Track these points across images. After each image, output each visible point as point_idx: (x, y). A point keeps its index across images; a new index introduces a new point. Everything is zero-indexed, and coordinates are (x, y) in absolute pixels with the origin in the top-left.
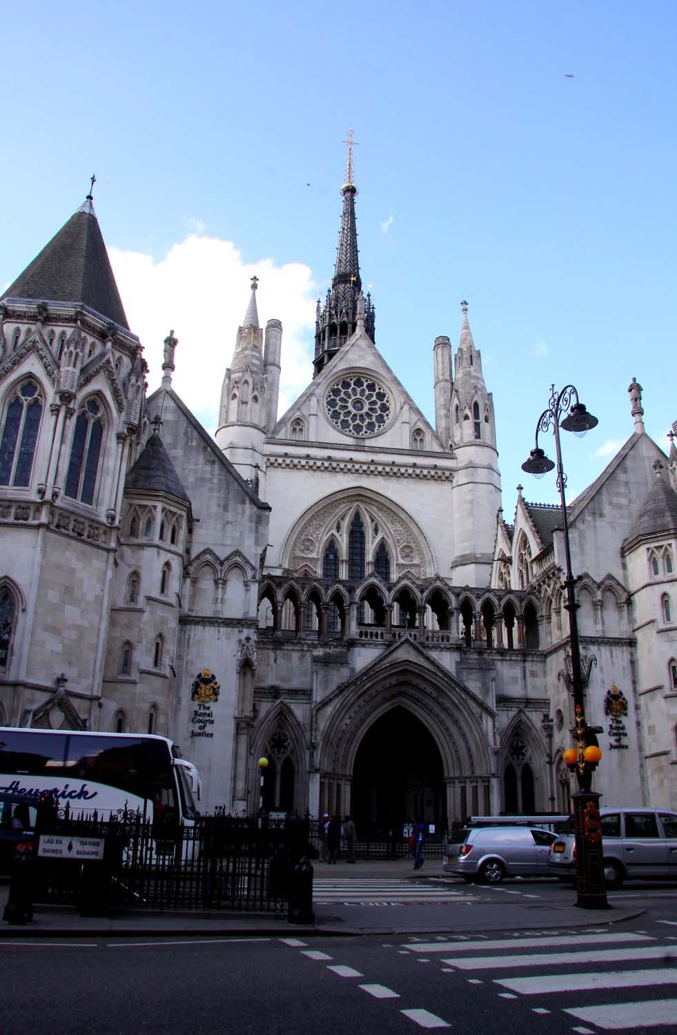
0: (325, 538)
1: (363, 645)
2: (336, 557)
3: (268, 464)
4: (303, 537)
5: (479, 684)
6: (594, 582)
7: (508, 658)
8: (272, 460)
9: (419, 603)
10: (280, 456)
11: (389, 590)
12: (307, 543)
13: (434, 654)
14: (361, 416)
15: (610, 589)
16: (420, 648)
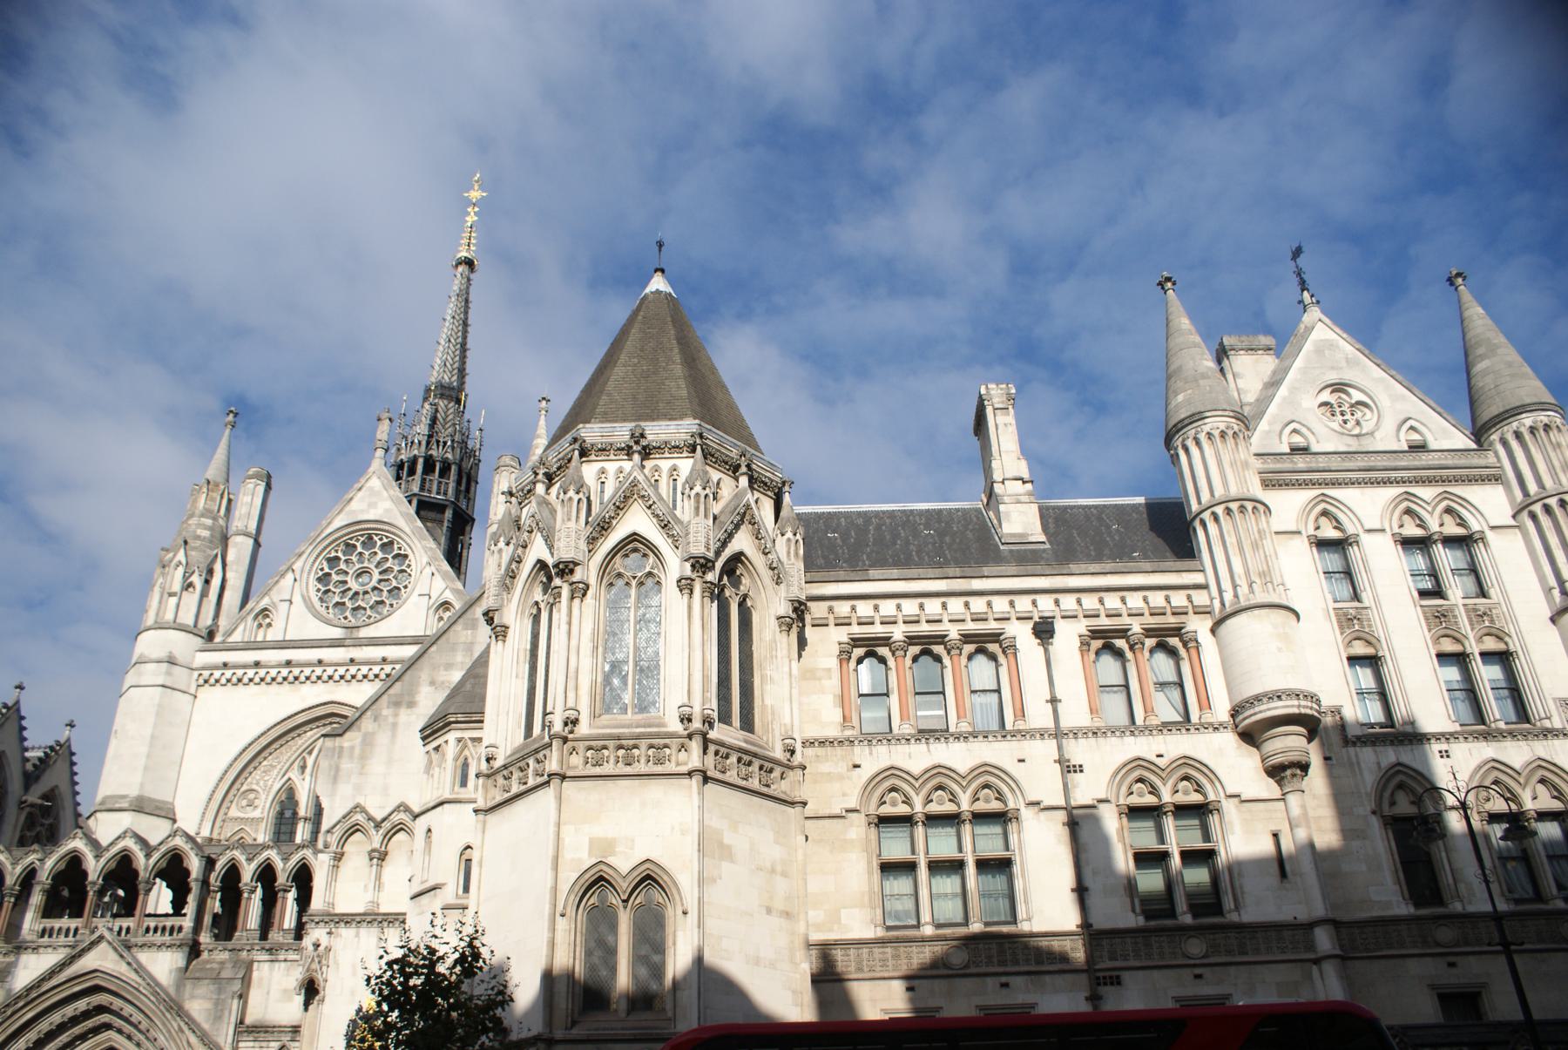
0: (277, 786)
1: (35, 949)
2: (295, 813)
3: (201, 681)
4: (245, 787)
5: (208, 1005)
6: (370, 818)
7: (281, 957)
8: (206, 673)
9: (143, 875)
10: (217, 668)
11: (97, 857)
12: (252, 796)
13: (144, 957)
14: (375, 588)
15: (399, 828)
16: (126, 947)
